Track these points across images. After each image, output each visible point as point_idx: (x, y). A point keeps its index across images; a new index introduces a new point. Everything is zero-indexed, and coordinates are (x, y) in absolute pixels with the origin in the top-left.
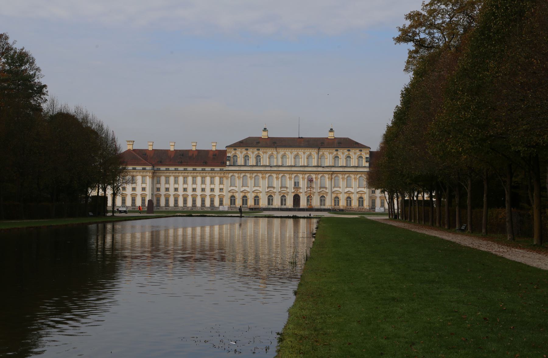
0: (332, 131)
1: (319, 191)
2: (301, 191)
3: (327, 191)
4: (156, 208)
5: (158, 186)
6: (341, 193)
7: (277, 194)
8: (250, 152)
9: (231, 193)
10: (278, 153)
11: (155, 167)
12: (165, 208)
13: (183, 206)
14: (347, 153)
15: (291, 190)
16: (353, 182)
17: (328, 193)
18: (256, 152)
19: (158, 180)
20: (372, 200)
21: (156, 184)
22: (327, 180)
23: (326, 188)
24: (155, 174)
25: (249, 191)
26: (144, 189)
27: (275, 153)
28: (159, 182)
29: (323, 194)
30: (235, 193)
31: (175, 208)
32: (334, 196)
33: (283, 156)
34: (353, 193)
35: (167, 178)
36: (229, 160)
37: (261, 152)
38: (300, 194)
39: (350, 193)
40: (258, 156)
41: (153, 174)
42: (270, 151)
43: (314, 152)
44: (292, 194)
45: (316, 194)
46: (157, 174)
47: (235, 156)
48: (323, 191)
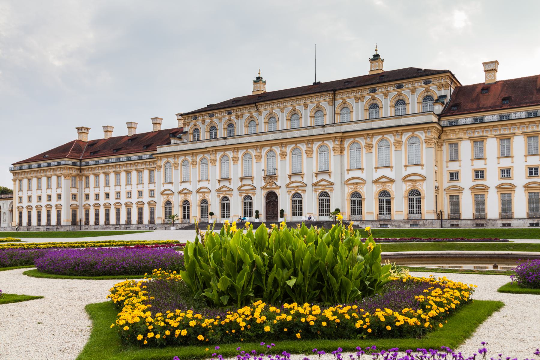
0: (377, 59)
1: (315, 181)
2: (279, 183)
3: (332, 180)
4: (84, 227)
5: (87, 191)
6: (364, 182)
7: (235, 192)
8: (216, 120)
9: (164, 197)
10: (260, 113)
11: (83, 161)
12: (93, 227)
13: (115, 223)
14: (393, 91)
15: (259, 182)
16: (393, 152)
17: (333, 184)
18: (225, 118)
19: (87, 181)
20: (450, 196)
21: (85, 188)
22: (332, 153)
23: (328, 172)
24: (83, 173)
25: (191, 189)
26: (59, 196)
27: (255, 114)
28: (87, 186)
29: (323, 187)
30: (171, 196)
31: (105, 227)
32: (349, 190)
33: (271, 117)
34: (392, 181)
35: (97, 176)
36: (180, 138)
37: (233, 117)
38: (277, 191)
39: (385, 182)
40: (231, 126)
41: (81, 172)
42: (247, 113)
43: (324, 102)
44: (263, 191)
45: (309, 188)
46: (86, 172)
47: (196, 130)
48: (323, 180)
